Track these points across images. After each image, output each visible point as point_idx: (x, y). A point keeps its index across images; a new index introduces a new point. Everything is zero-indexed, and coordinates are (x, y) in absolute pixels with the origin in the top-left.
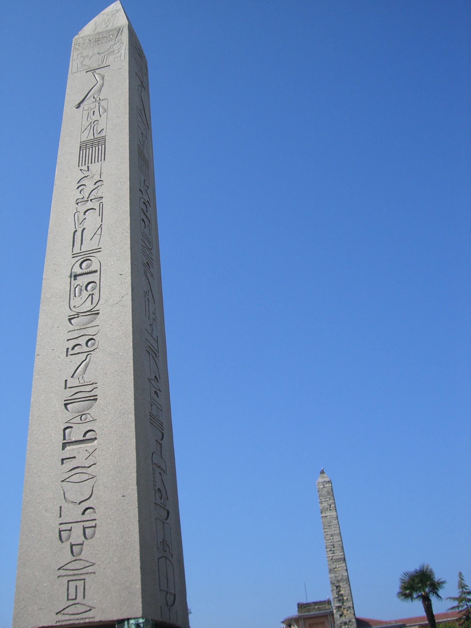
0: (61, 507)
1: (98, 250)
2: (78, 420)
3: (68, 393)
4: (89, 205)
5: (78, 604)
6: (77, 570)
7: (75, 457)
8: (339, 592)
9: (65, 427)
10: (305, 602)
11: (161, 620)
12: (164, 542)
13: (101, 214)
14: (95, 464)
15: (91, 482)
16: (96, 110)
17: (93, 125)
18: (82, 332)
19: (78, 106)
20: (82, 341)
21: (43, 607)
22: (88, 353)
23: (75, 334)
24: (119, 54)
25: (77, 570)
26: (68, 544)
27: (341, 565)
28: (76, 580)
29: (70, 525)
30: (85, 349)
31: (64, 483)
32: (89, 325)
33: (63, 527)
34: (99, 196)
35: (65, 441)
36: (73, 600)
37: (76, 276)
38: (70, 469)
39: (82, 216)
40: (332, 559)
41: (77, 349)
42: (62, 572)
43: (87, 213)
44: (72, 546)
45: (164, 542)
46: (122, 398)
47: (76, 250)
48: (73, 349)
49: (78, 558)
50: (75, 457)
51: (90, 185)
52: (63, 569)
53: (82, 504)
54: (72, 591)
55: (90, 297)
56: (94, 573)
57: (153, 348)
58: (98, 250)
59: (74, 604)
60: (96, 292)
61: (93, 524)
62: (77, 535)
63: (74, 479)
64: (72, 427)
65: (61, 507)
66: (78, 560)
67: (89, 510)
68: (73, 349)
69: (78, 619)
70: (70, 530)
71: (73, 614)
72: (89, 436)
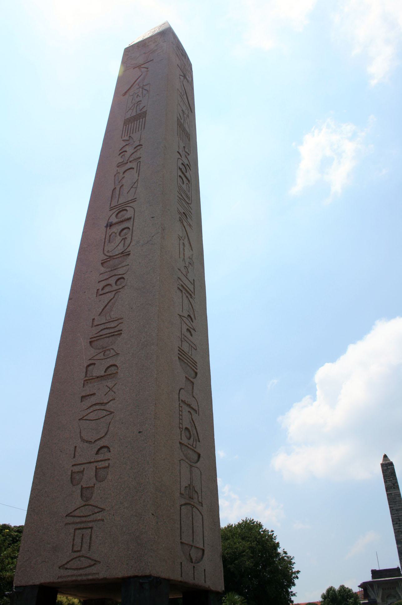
0: (76, 447)
1: (134, 200)
2: (101, 356)
4: (129, 165)
5: (83, 556)
6: (86, 516)
7: (94, 394)
9: (89, 363)
10: (377, 569)
11: (180, 579)
12: (190, 487)
14: (114, 399)
17: (136, 105)
18: (113, 273)
19: (125, 94)
20: (112, 281)
21: (47, 560)
22: (117, 291)
25: (86, 516)
26: (80, 486)
28: (83, 528)
29: (83, 466)
30: (115, 287)
31: (81, 421)
32: (120, 266)
33: (76, 469)
34: (137, 157)
35: (87, 378)
36: (78, 551)
37: (111, 226)
38: (89, 406)
39: (121, 175)
41: (107, 289)
42: (70, 520)
43: (126, 173)
44: (82, 488)
45: (190, 487)
46: (146, 330)
47: (114, 203)
48: (102, 289)
49: (87, 503)
50: (94, 394)
51: (130, 150)
52: (71, 516)
53: (97, 442)
55: (123, 242)
56: (103, 520)
57: (189, 290)
58: (134, 200)
59: (79, 556)
60: (129, 236)
61: (106, 464)
64: (94, 364)
65: (76, 447)
66: (88, 505)
67: (103, 449)
68: (102, 289)
69: (80, 575)
70: (82, 472)
71: (77, 569)
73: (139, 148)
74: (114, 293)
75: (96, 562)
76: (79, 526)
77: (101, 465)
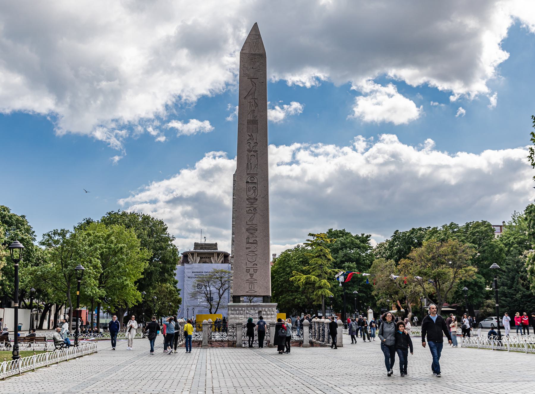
3: (248, 227)
4: (252, 153)
15: (256, 256)
16: (253, 103)
23: (249, 206)
41: (250, 212)
54: (250, 286)
60: (256, 191)
63: (250, 254)
72: (255, 241)
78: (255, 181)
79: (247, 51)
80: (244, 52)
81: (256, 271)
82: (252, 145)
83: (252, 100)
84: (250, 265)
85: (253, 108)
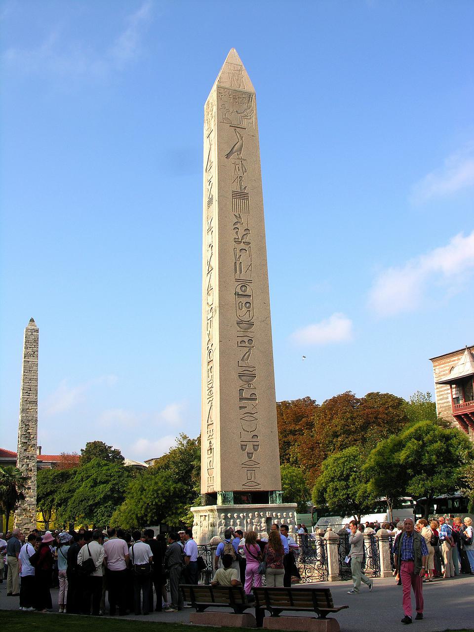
1: (250, 282)
3: (240, 370)
4: (242, 246)
8: (27, 430)
13: (250, 255)
17: (239, 180)
19: (228, 156)
23: (241, 334)
24: (250, 121)
27: (34, 408)
32: (249, 330)
33: (243, 443)
40: (26, 400)
58: (250, 282)
62: (250, 448)
73: (247, 232)
74: (248, 348)
75: (259, 484)
76: (250, 469)
77: (255, 443)
78: (248, 292)
79: (227, 85)
80: (222, 85)
81: (255, 447)
82: (241, 232)
83: (237, 161)
84: (247, 437)
85: (240, 173)
